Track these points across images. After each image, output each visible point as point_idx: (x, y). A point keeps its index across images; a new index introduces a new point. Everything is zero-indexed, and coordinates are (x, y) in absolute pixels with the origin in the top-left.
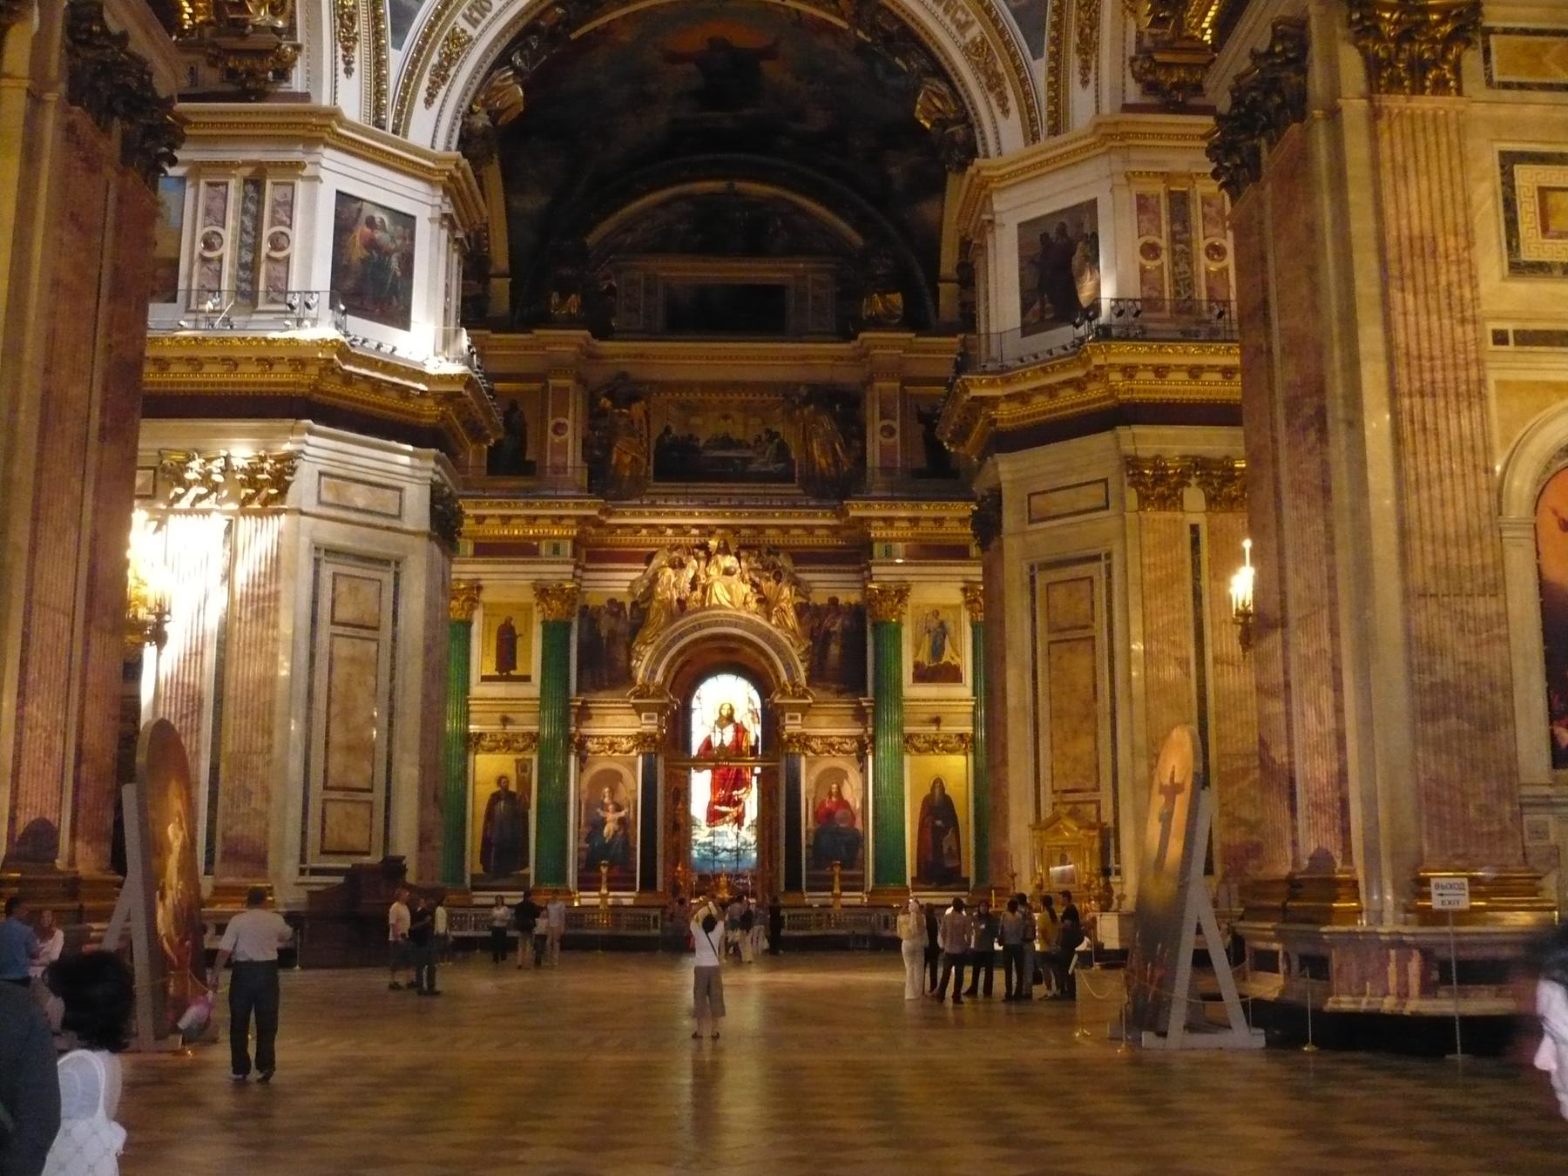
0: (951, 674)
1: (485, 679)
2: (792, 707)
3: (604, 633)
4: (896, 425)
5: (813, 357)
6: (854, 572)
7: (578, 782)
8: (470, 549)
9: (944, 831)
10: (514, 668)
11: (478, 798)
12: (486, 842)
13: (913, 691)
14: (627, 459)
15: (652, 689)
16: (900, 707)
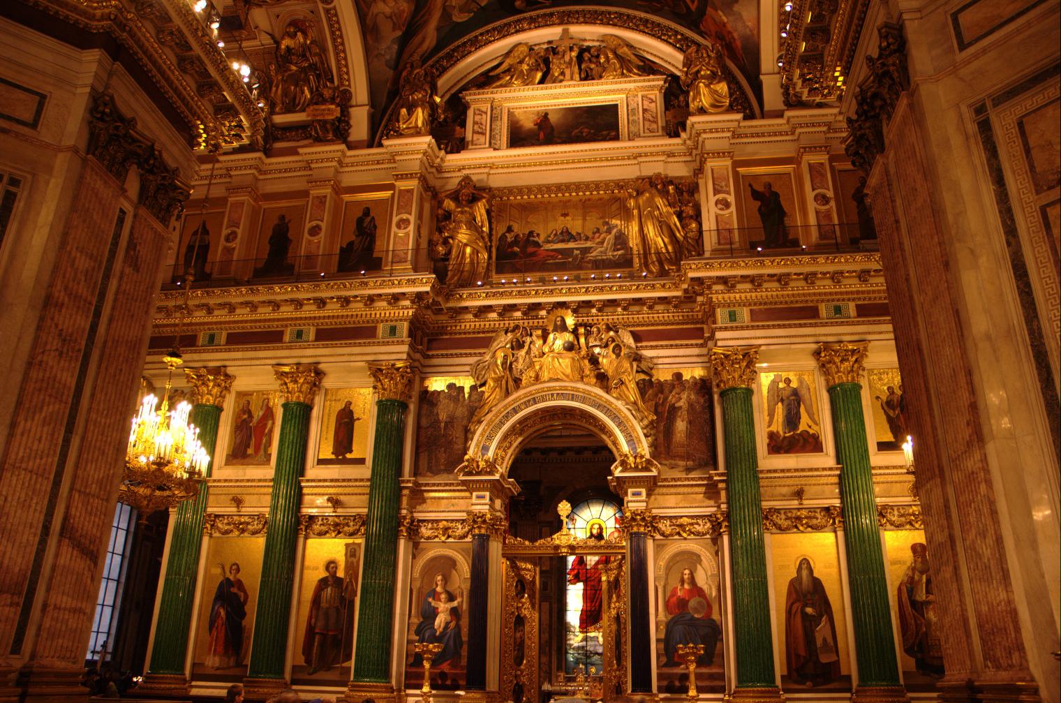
0: (812, 444)
1: (321, 462)
2: (635, 481)
3: (443, 416)
4: (731, 199)
5: (646, 155)
6: (697, 345)
7: (410, 569)
8: (312, 336)
9: (815, 620)
10: (351, 451)
11: (305, 581)
12: (310, 631)
13: (767, 461)
14: (468, 250)
15: (482, 464)
16: (757, 479)
